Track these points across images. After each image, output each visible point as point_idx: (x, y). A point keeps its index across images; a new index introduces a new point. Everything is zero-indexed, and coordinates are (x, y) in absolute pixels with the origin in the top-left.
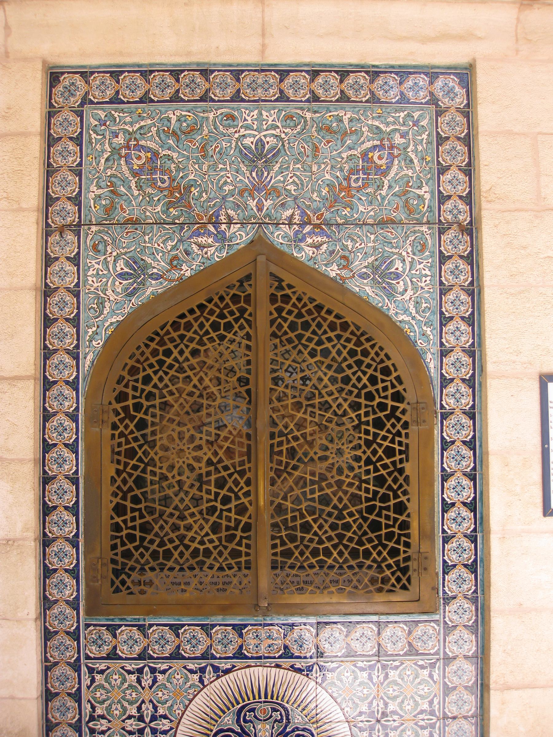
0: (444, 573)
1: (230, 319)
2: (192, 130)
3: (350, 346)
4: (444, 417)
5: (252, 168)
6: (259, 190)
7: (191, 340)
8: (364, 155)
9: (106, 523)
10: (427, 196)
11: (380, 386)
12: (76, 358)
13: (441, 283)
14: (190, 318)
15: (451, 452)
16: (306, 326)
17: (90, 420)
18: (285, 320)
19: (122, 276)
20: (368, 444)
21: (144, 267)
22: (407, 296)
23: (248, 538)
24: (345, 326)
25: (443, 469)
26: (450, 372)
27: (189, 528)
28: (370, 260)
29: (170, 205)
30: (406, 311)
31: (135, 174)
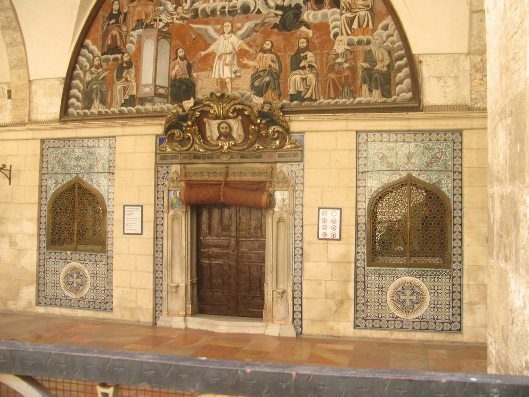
2: (67, 153)
5: (77, 161)
6: (77, 165)
8: (96, 158)
10: (107, 167)
17: (48, 211)
19: (54, 183)
21: (58, 182)
24: (91, 194)
29: (62, 169)
31: (57, 162)
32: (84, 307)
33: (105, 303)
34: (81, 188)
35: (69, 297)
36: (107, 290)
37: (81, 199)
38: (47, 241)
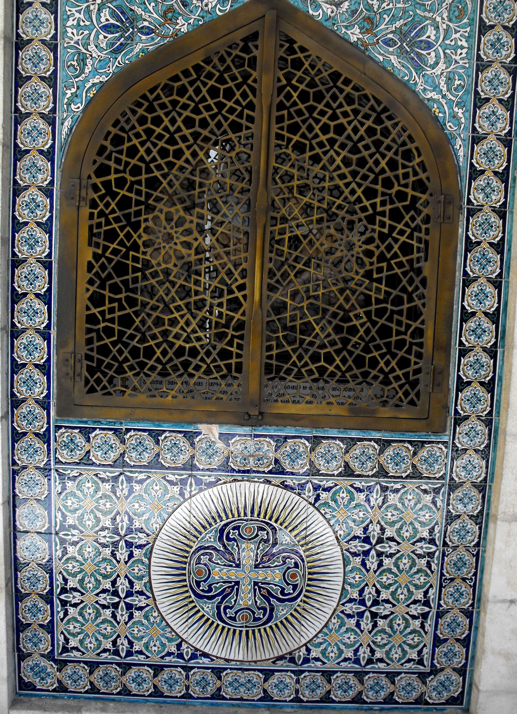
0: (459, 390)
1: (231, 84)
3: (369, 123)
4: (471, 213)
7: (185, 107)
9: (81, 313)
11: (401, 171)
12: (52, 123)
13: (479, 57)
14: (185, 81)
15: (476, 253)
16: (319, 97)
17: (67, 196)
18: (295, 89)
19: (107, 28)
20: (383, 237)
21: (133, 19)
22: (438, 71)
23: (241, 337)
25: (465, 273)
26: (480, 163)
27: (173, 322)
28: (398, 24)
30: (436, 88)
32: (297, 700)
33: (423, 677)
34: (297, 64)
35: (205, 655)
36: (439, 615)
37: (294, 129)
38: (63, 362)
